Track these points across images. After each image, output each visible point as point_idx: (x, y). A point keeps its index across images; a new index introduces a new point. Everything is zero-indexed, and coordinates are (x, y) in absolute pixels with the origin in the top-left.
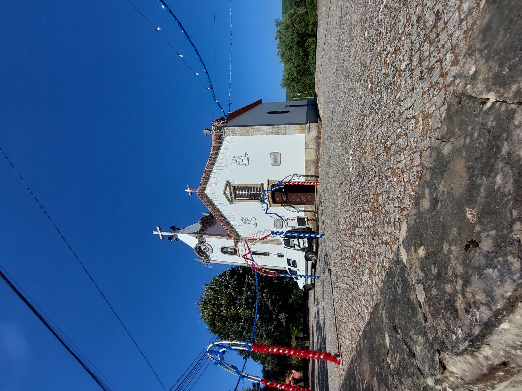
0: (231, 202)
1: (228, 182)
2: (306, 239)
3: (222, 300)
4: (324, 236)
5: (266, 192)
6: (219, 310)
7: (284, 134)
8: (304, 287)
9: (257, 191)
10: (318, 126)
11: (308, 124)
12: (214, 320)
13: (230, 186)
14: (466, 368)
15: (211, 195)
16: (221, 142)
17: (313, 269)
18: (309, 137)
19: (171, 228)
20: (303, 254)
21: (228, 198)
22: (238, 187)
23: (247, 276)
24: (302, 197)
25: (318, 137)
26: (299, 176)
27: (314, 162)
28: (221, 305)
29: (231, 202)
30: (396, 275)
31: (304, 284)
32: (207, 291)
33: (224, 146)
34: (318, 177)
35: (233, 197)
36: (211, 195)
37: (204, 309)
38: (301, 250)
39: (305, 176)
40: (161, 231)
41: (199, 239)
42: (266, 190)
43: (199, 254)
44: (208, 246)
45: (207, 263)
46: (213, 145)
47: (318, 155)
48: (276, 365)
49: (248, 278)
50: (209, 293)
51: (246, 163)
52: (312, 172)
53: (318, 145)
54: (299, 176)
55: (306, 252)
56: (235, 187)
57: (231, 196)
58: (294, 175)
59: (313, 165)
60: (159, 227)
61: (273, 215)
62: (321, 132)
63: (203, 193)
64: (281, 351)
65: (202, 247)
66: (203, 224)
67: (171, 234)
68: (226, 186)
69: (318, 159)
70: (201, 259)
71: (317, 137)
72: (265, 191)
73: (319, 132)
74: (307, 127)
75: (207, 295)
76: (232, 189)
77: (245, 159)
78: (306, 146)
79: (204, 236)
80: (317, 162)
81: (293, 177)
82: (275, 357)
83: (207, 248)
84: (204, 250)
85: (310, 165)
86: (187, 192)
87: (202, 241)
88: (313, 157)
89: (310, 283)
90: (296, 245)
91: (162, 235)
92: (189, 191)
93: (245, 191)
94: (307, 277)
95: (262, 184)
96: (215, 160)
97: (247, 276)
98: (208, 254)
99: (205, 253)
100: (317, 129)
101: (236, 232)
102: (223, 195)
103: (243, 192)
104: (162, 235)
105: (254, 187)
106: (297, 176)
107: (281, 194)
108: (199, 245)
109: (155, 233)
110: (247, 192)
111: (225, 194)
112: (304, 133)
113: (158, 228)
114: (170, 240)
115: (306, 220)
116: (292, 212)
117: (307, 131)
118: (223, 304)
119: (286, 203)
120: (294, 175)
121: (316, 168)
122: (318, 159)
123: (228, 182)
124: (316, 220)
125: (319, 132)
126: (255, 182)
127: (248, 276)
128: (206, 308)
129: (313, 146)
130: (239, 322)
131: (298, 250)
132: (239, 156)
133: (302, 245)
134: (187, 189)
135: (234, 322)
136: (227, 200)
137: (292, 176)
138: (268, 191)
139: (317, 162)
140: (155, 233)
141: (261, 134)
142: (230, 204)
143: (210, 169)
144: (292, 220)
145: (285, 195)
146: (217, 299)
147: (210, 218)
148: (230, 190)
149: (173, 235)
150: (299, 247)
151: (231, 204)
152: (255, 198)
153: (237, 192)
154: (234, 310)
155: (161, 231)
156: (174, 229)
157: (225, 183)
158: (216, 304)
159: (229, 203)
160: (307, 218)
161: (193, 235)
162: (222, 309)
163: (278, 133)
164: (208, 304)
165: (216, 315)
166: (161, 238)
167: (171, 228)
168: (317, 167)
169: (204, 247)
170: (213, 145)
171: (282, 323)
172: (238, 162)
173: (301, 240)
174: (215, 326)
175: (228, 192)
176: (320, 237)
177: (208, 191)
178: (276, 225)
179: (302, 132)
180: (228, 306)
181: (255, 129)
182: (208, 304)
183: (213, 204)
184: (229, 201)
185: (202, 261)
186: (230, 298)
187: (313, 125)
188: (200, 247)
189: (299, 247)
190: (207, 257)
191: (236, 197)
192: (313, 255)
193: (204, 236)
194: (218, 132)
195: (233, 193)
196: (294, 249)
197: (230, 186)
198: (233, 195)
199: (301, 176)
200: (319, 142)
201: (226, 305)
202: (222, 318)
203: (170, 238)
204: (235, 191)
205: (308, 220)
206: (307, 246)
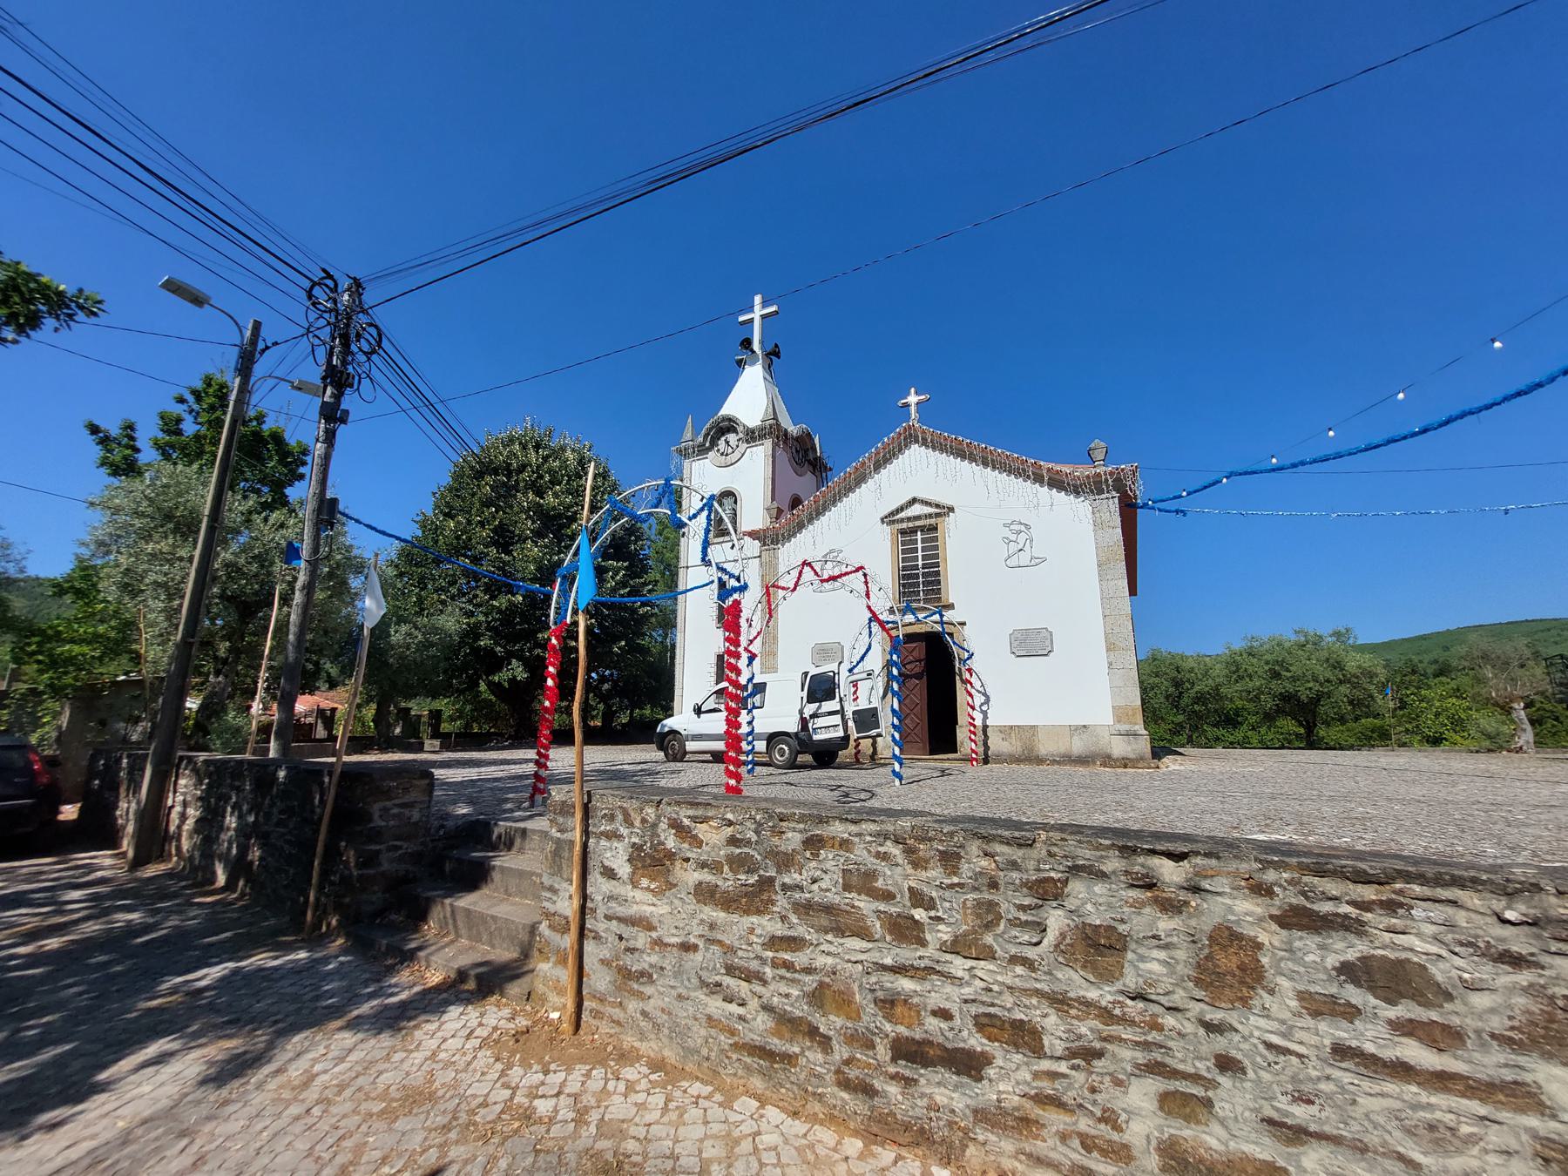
0: (889, 519)
1: (951, 509)
2: (841, 733)
3: (556, 495)
4: (897, 782)
5: (936, 617)
6: (526, 489)
7: (1110, 664)
8: (674, 732)
9: (926, 592)
10: (1142, 759)
11: (1146, 732)
12: (495, 472)
13: (938, 515)
14: (1535, 1008)
15: (907, 462)
16: (1076, 490)
17: (708, 757)
18: (1106, 735)
19: (776, 346)
20: (792, 726)
21: (901, 509)
22: (936, 539)
23: (626, 564)
24: (919, 720)
25: (1108, 760)
26: (984, 708)
27: (1032, 750)
28: (540, 493)
29: (889, 519)
30: (1503, 903)
31: (683, 732)
32: (573, 450)
33: (1061, 497)
34: (986, 761)
35: (904, 525)
36: (907, 462)
37: (520, 443)
38: (804, 722)
39: (985, 727)
40: (763, 317)
41: (762, 429)
42: (945, 619)
43: (711, 429)
44: (737, 455)
45: (684, 454)
46: (1066, 469)
47: (1054, 762)
48: (402, 657)
49: (620, 569)
50: (569, 454)
51: (1013, 561)
52: (997, 744)
53: (1083, 760)
54: (984, 708)
55: (796, 734)
56: (934, 528)
57: (909, 519)
58: (985, 694)
59: (1020, 749)
60: (776, 313)
61: (867, 640)
62: (1125, 767)
63: (910, 438)
64: (551, 669)
65: (732, 437)
66: (797, 439)
67: (756, 346)
68: (937, 506)
69: (1040, 761)
70: (696, 433)
71: (1109, 757)
72: (942, 616)
73: (1125, 763)
74: (1137, 727)
75: (563, 449)
76: (928, 522)
77: (1024, 558)
78: (1077, 728)
79: (768, 443)
80: (1030, 757)
81: (979, 692)
82: (422, 654)
83: (730, 450)
84: (722, 442)
85: (1021, 739)
86: (909, 394)
87: (752, 436)
88: (1045, 747)
89: (688, 749)
90: (819, 707)
91: (751, 321)
92: (913, 399)
93: (924, 557)
94: (750, 738)
95: (951, 607)
96: (1019, 472)
97: (626, 564)
98: (711, 454)
99: (714, 443)
100: (1132, 756)
101: (794, 535)
102: (909, 497)
103: (920, 554)
104: (751, 321)
105: (939, 582)
106: (982, 705)
107: (920, 661)
108: (740, 429)
109: (758, 299)
110: (920, 563)
111: (914, 501)
112: (1118, 720)
113: (773, 309)
114: (742, 344)
115: (873, 732)
116: (868, 693)
117: (1124, 727)
118: (543, 498)
119: (899, 677)
120: (985, 694)
121: (1011, 756)
122: (1040, 761)
123: (951, 509)
124: (858, 761)
125: (1125, 763)
126: (955, 587)
127: (626, 569)
128: (524, 447)
129: (1078, 746)
130: (495, 543)
131: (801, 712)
132: (1032, 541)
133: (820, 722)
134: (916, 393)
135: (495, 531)
136: (894, 507)
137: (981, 689)
138: (942, 623)
139: (1030, 757)
140: (758, 299)
141: (1105, 599)
142: (882, 515)
143: (993, 460)
144: (855, 693)
145: (917, 670)
146: (554, 482)
147: (811, 457)
148: (930, 516)
149: (753, 352)
150: (814, 716)
151: (882, 520)
152: (904, 586)
153: (919, 536)
154: (532, 531)
155: (763, 317)
156: (773, 354)
157: (945, 501)
158: (541, 477)
159: (886, 512)
160: (879, 735)
161: (770, 410)
162: (531, 496)
163: (1110, 647)
164: (537, 452)
165: (509, 476)
166: (741, 319)
167: (776, 346)
168: (1018, 760)
169: (733, 442)
170: (1066, 469)
171: (499, 669)
172: (1013, 537)
173: (837, 719)
174: (479, 475)
175: (917, 510)
176: (894, 771)
177: (916, 454)
178: (825, 647)
179: (1120, 714)
180: (541, 513)
181: (1120, 582)
182: (537, 452)
183: (878, 466)
184: (892, 514)
185: (688, 435)
186: (560, 516)
187: (1143, 745)
188: (734, 430)
189: (814, 716)
190: (702, 450)
191: (903, 532)
192: (787, 755)
193: (768, 443)
194: (1106, 480)
195: (918, 523)
196: (805, 700)
197: (938, 515)
198: (911, 525)
199: (985, 714)
200: (1094, 763)
201: (542, 506)
202: (506, 493)
203: (747, 344)
204: (923, 529)
205: (874, 737)
206: (815, 737)
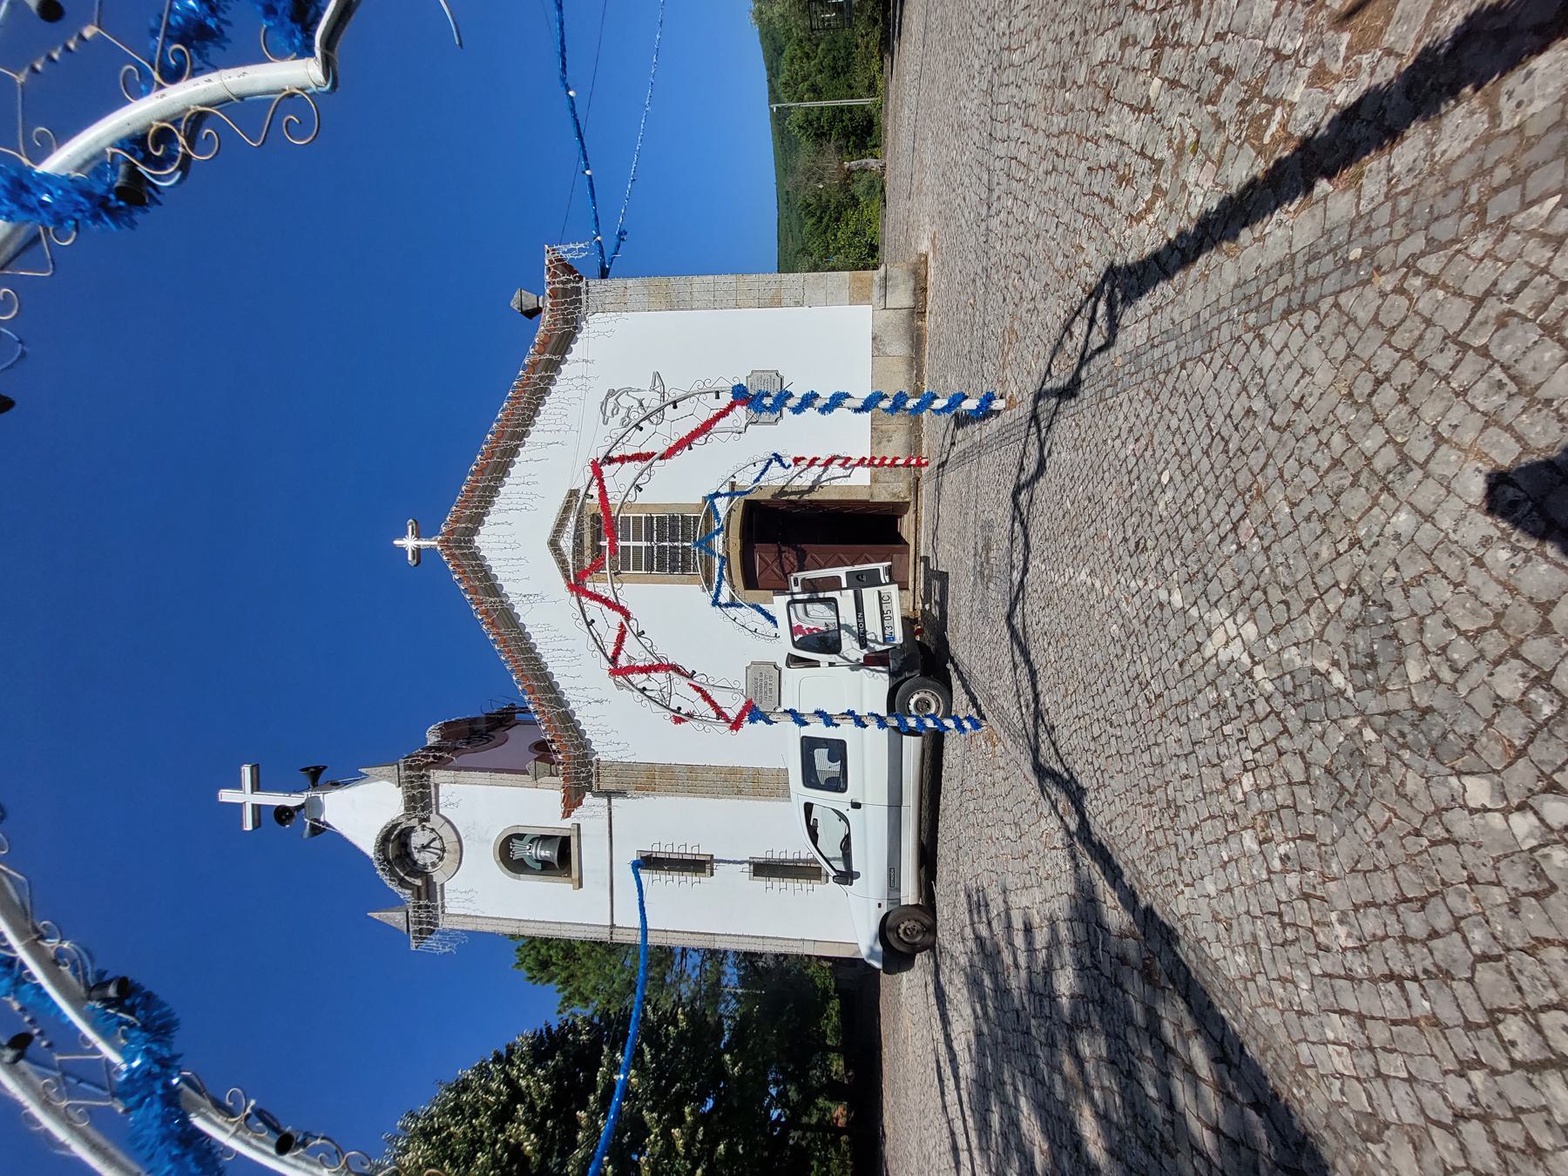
7: (798, 304)
21: (562, 562)
25: (917, 312)
31: (884, 910)
38: (873, 660)
40: (257, 786)
43: (393, 873)
44: (446, 832)
45: (427, 927)
53: (917, 341)
55: (892, 674)
60: (256, 770)
63: (463, 542)
65: (418, 839)
66: (444, 738)
74: (876, 278)
84: (423, 858)
87: (420, 801)
90: (848, 628)
97: (606, 1049)
98: (438, 877)
99: (421, 872)
100: (911, 284)
101: (581, 734)
105: (673, 518)
107: (780, 552)
109: (227, 796)
110: (644, 544)
111: (554, 545)
113: (246, 771)
114: (282, 822)
117: (876, 292)
121: (911, 431)
129: (899, 348)
131: (856, 666)
133: (873, 627)
140: (227, 796)
141: (715, 304)
149: (302, 806)
150: (863, 641)
155: (257, 786)
156: (316, 777)
163: (776, 302)
175: (567, 543)
179: (859, 296)
185: (396, 918)
188: (406, 834)
190: (428, 892)
193: (437, 776)
194: (563, 283)
198: (588, 552)
203: (283, 814)
206: (899, 638)
